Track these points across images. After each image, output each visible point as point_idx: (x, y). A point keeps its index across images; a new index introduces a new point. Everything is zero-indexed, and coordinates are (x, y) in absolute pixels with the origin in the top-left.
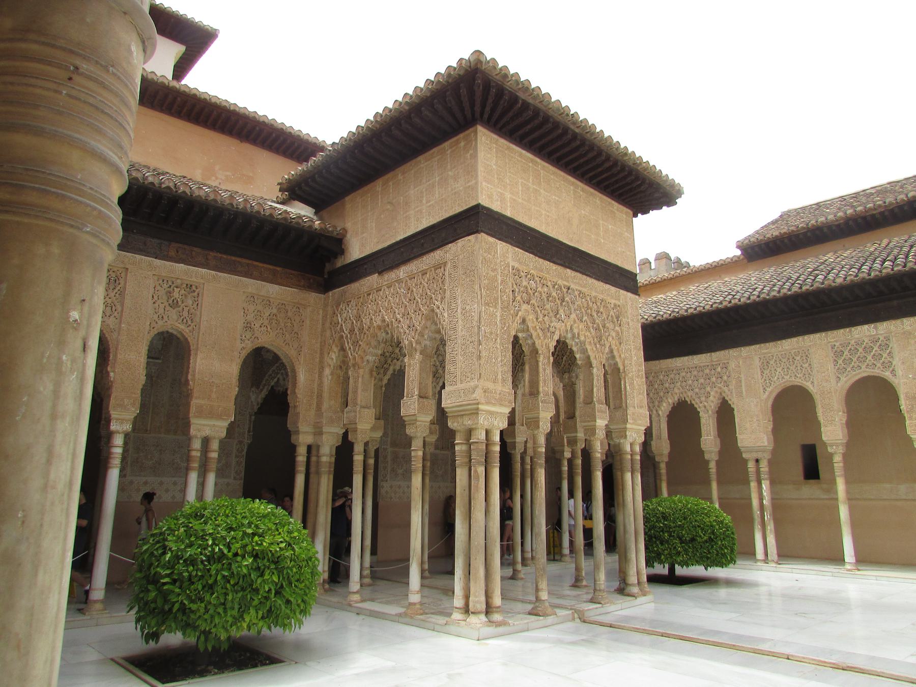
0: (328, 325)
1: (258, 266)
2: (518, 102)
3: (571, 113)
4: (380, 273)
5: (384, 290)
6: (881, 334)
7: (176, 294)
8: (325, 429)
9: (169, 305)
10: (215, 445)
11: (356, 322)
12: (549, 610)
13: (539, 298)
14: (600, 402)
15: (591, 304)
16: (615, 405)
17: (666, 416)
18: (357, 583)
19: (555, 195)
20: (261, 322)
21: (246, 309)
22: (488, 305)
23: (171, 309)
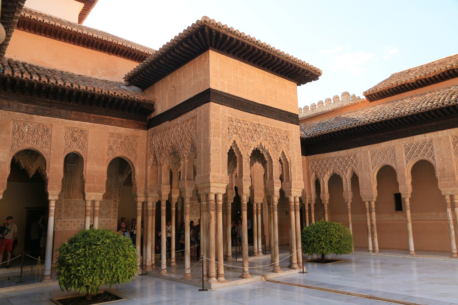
0: (149, 145)
1: (114, 119)
2: (228, 38)
3: (256, 40)
4: (170, 121)
5: (172, 129)
6: (428, 139)
7: (75, 135)
8: (149, 195)
10: (97, 204)
12: (249, 276)
13: (242, 131)
14: (276, 178)
15: (272, 132)
16: (286, 179)
17: (327, 181)
18: (165, 265)
20: (116, 146)
21: (109, 140)
22: (215, 136)
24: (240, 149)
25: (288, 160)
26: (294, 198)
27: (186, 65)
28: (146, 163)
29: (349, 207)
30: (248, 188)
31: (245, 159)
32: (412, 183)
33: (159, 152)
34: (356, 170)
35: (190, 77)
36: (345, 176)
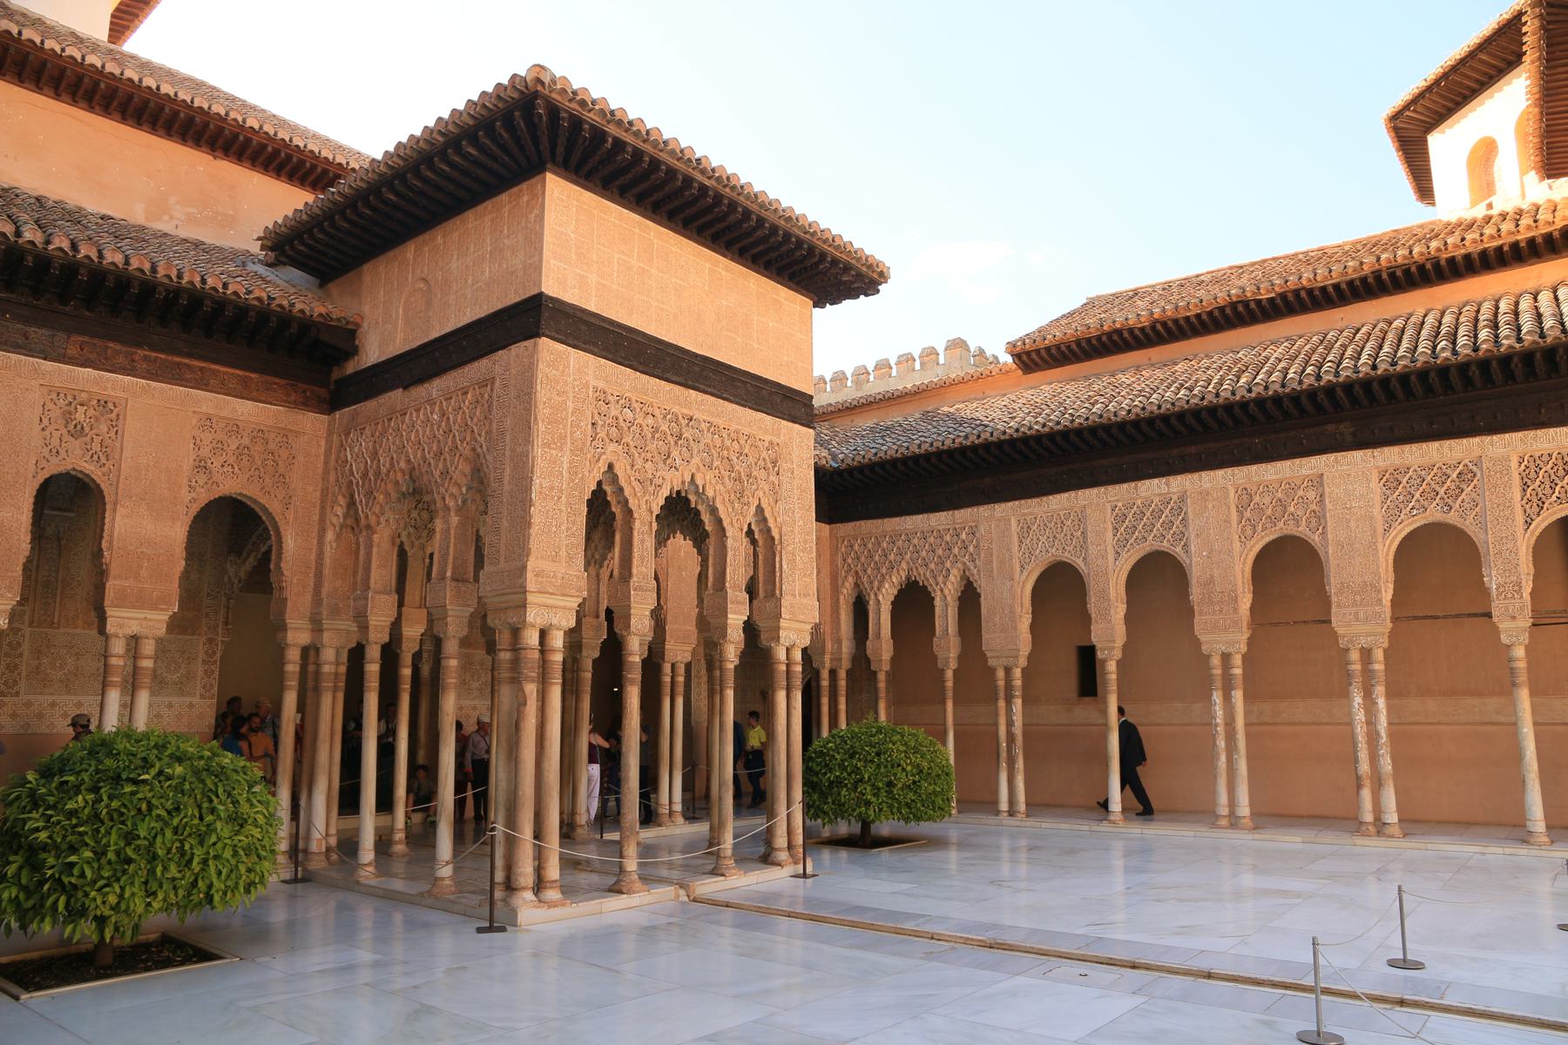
0: (332, 463)
1: (218, 371)
2: (607, 141)
3: (696, 157)
4: (406, 388)
5: (411, 414)
8: (326, 623)
9: (69, 431)
10: (148, 648)
11: (372, 461)
12: (638, 885)
14: (734, 587)
15: (728, 443)
19: (677, 277)
20: (222, 459)
21: (198, 439)
23: (72, 439)
24: (627, 493)
25: (775, 533)
26: (788, 649)
27: (470, 214)
28: (322, 521)
29: (950, 684)
30: (647, 613)
31: (643, 523)
32: (1128, 618)
33: (366, 486)
34: (975, 572)
35: (480, 253)
36: (942, 590)
